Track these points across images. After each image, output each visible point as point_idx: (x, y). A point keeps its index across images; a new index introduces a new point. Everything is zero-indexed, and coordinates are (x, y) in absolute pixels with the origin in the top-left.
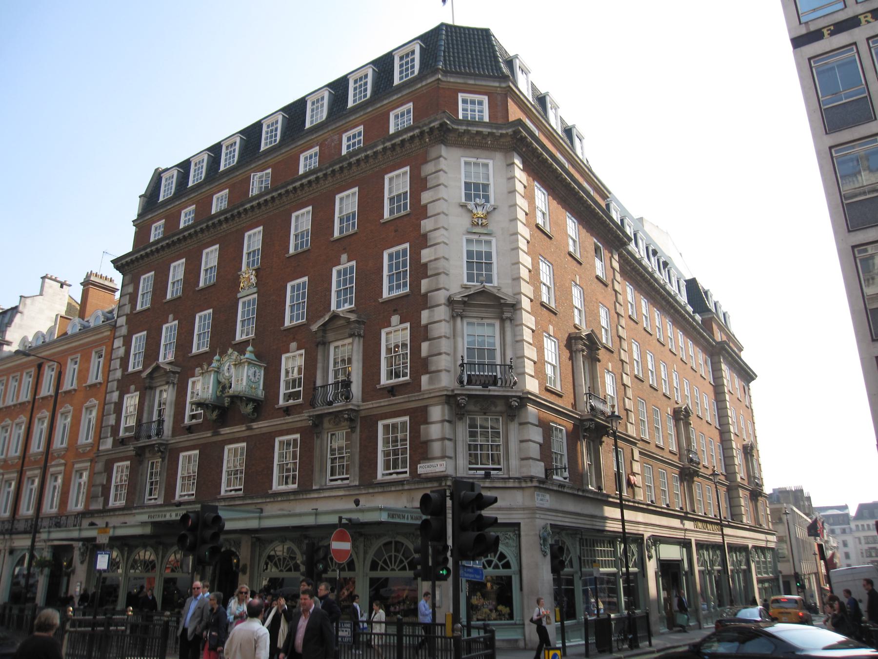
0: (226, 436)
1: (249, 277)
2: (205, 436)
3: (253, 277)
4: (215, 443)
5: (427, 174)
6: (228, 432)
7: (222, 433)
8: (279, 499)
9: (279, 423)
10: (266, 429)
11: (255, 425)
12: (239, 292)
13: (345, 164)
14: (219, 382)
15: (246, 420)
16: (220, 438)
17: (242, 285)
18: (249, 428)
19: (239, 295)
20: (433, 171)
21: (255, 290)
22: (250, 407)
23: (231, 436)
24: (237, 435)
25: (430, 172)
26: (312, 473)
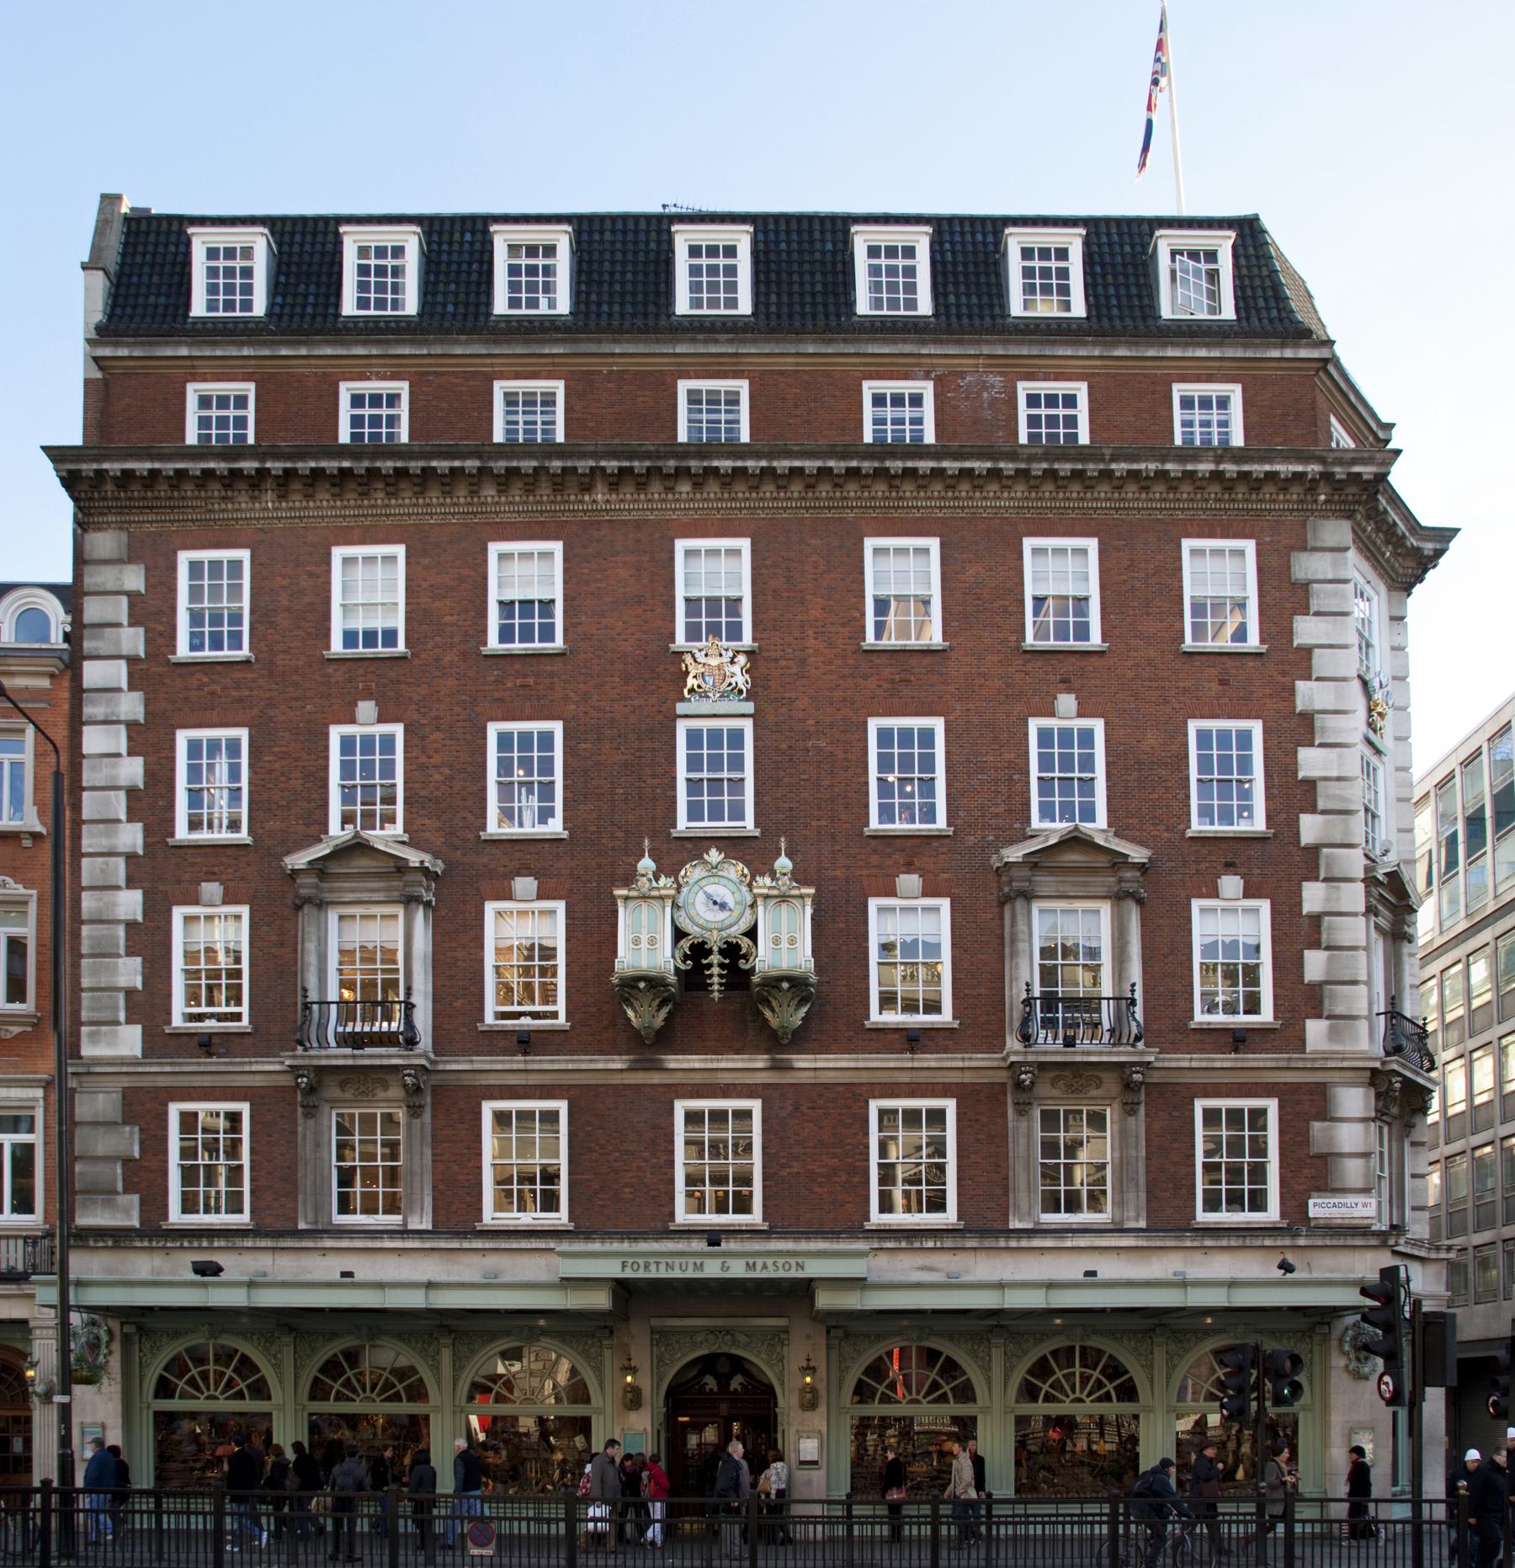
0: (679, 1075)
1: (720, 667)
2: (601, 1066)
3: (736, 669)
4: (637, 1088)
5: (1310, 576)
6: (697, 1065)
7: (672, 1065)
8: (930, 1244)
9: (892, 1065)
10: (831, 1074)
11: (802, 1061)
12: (683, 699)
13: (1007, 466)
14: (679, 934)
15: (776, 1043)
16: (655, 1078)
17: (691, 682)
18: (776, 1067)
19: (681, 708)
20: (1330, 577)
21: (749, 707)
22: (797, 1017)
23: (697, 1078)
24: (727, 1078)
25: (1320, 576)
26: (1006, 1194)
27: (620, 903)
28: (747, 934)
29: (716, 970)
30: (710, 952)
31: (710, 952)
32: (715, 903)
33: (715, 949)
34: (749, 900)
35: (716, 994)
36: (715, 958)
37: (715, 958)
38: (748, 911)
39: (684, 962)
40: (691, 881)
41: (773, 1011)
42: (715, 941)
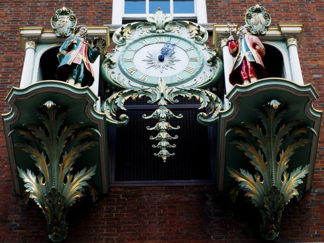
27: (29, 45)
28: (204, 88)
29: (163, 125)
30: (156, 105)
31: (156, 105)
32: (161, 59)
33: (163, 102)
34: (208, 55)
35: (165, 152)
36: (162, 112)
37: (162, 112)
38: (207, 68)
39: (117, 118)
40: (128, 42)
41: (253, 171)
42: (162, 93)
